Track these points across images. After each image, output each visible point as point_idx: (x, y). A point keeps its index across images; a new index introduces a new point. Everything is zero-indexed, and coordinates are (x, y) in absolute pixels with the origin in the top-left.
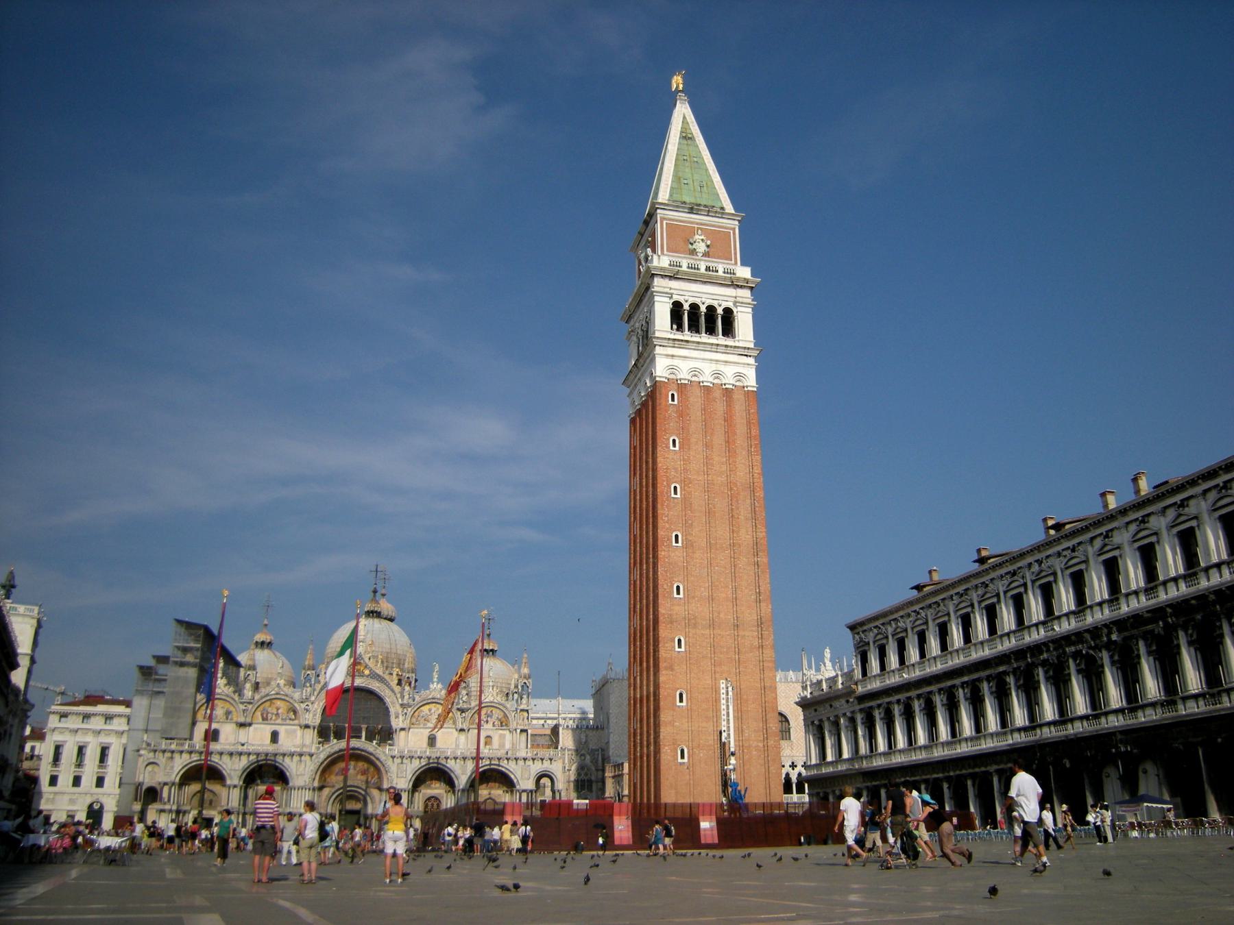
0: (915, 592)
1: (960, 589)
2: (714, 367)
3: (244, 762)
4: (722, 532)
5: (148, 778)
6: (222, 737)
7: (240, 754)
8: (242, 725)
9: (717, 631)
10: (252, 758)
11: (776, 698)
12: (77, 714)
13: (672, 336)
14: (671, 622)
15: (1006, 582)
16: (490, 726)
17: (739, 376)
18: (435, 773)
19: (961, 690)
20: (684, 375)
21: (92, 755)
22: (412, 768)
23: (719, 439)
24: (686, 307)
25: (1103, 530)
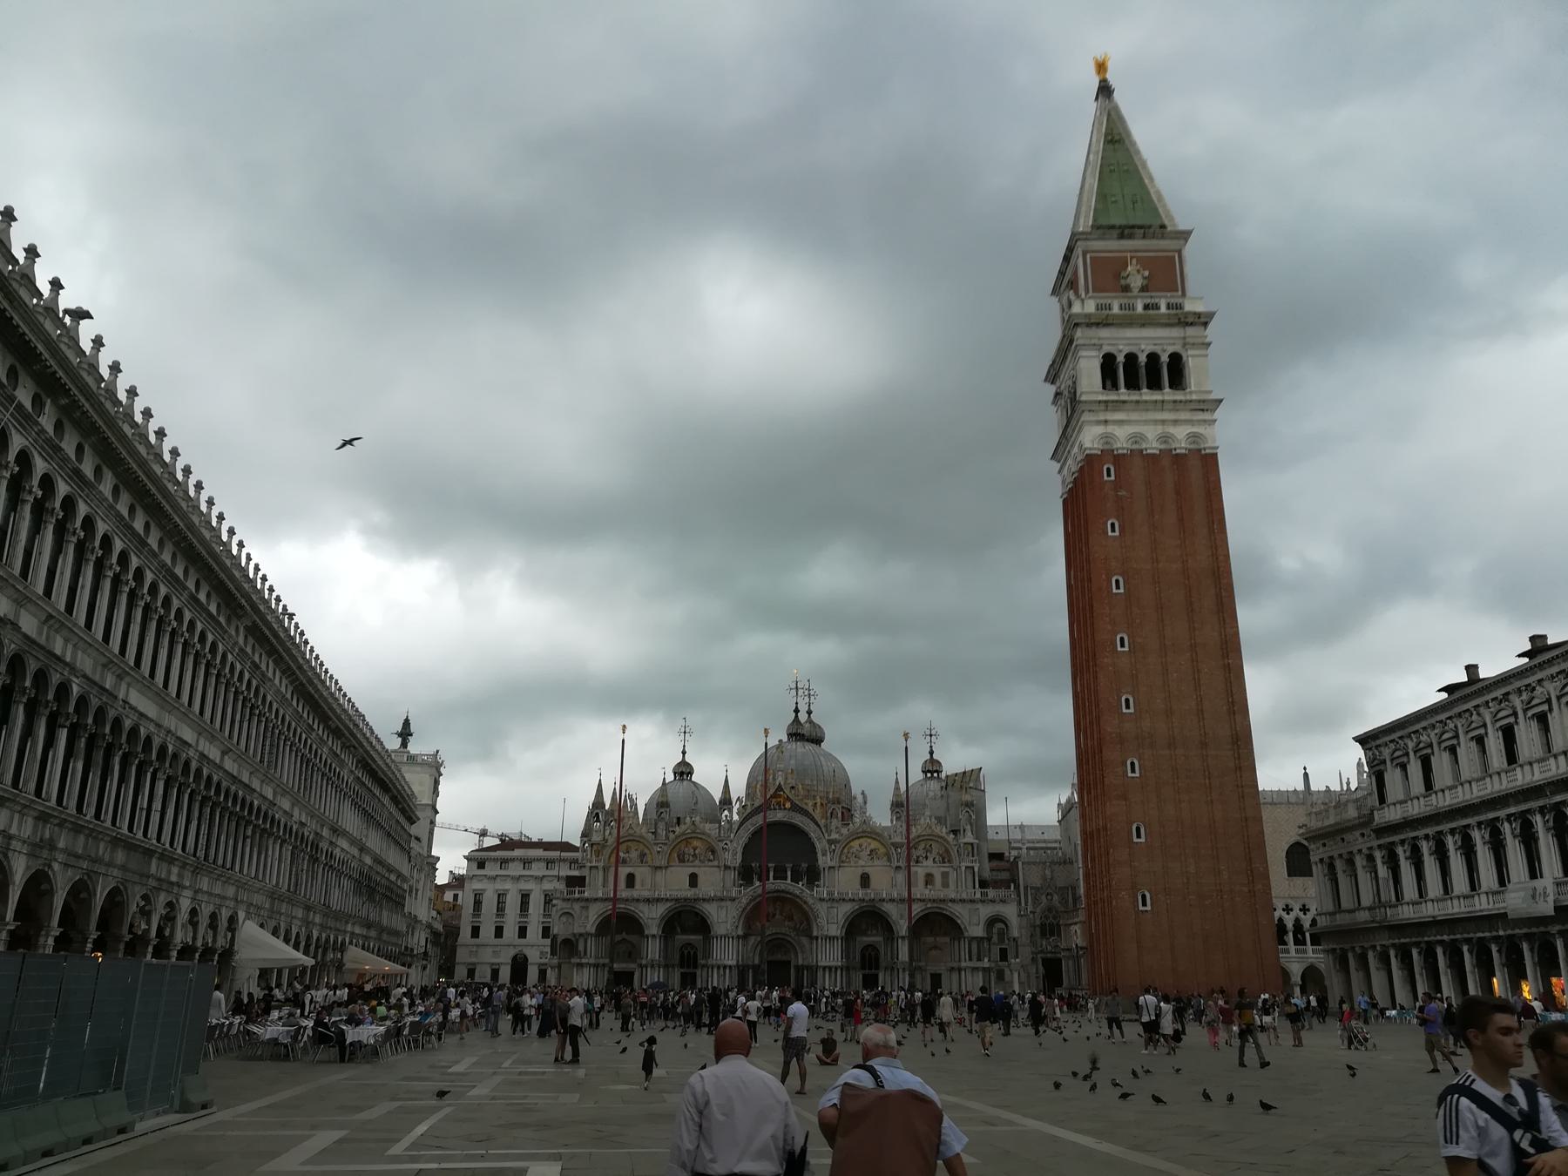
0: (1444, 695)
1: (1499, 693)
2: (1160, 429)
3: (660, 910)
7: (658, 900)
13: (1104, 398)
15: (1559, 684)
16: (930, 862)
17: (1194, 437)
18: (868, 918)
19: (1506, 825)
21: (513, 902)
22: (845, 909)
24: (1121, 359)
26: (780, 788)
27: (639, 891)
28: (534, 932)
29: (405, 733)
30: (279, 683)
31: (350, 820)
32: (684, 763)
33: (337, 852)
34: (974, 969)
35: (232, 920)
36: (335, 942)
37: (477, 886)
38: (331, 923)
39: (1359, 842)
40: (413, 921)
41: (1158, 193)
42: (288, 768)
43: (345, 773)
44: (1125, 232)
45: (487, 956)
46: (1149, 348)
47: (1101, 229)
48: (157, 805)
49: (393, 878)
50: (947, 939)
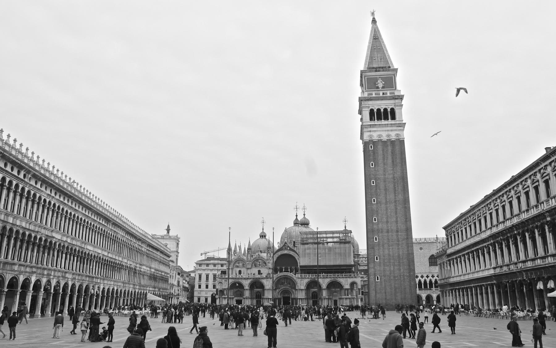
1: (464, 219)
3: (249, 281)
4: (391, 196)
6: (242, 272)
7: (248, 279)
8: (248, 269)
9: (390, 234)
11: (413, 257)
13: (370, 124)
14: (373, 232)
20: (375, 137)
21: (211, 278)
22: (306, 281)
23: (390, 161)
24: (375, 111)
25: (488, 202)
26: (286, 243)
27: (244, 275)
29: (168, 230)
30: (121, 233)
31: (145, 260)
32: (263, 232)
33: (142, 270)
34: (346, 298)
37: (200, 272)
38: (142, 288)
39: (445, 259)
41: (389, 55)
42: (126, 252)
43: (143, 249)
44: (377, 69)
45: (203, 294)
48: (94, 268)
49: (163, 274)
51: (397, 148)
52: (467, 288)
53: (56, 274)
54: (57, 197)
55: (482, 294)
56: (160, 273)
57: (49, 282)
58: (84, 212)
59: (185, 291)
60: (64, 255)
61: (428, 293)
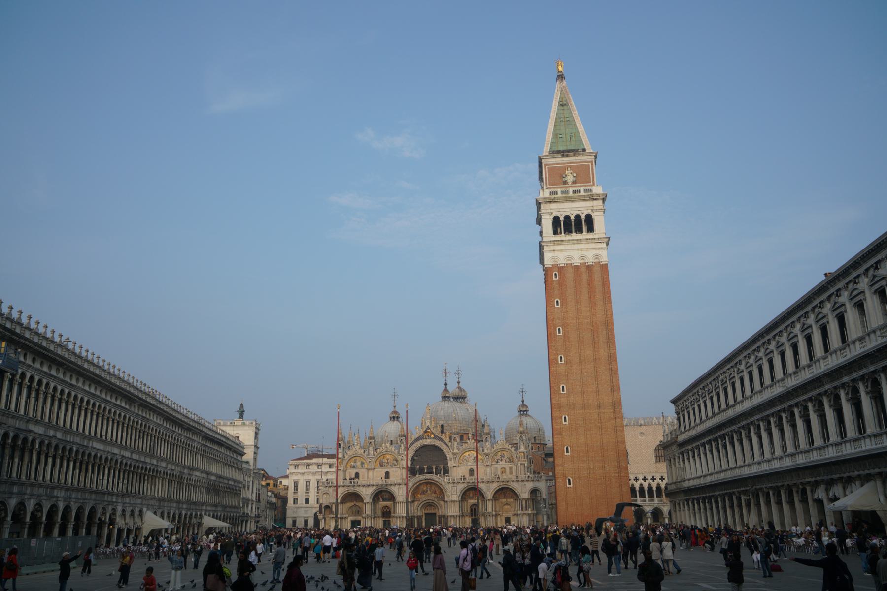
1: (701, 386)
2: (580, 253)
3: (371, 490)
5: (324, 501)
9: (587, 411)
10: (375, 487)
12: (303, 464)
14: (560, 408)
16: (503, 462)
17: (597, 256)
18: (472, 491)
20: (562, 262)
21: (313, 486)
22: (461, 487)
23: (585, 297)
24: (562, 219)
25: (737, 360)
26: (428, 428)
28: (313, 501)
35: (141, 512)
36: (196, 515)
37: (295, 478)
40: (247, 501)
44: (565, 153)
46: (575, 213)
47: (553, 153)
48: (106, 477)
49: (231, 483)
50: (512, 500)
51: (597, 276)
52: (710, 498)
53: (36, 490)
54: (37, 365)
55: (732, 507)
56: (226, 481)
57: (22, 505)
58: (86, 388)
59: (270, 509)
60: (50, 460)
61: (656, 506)
